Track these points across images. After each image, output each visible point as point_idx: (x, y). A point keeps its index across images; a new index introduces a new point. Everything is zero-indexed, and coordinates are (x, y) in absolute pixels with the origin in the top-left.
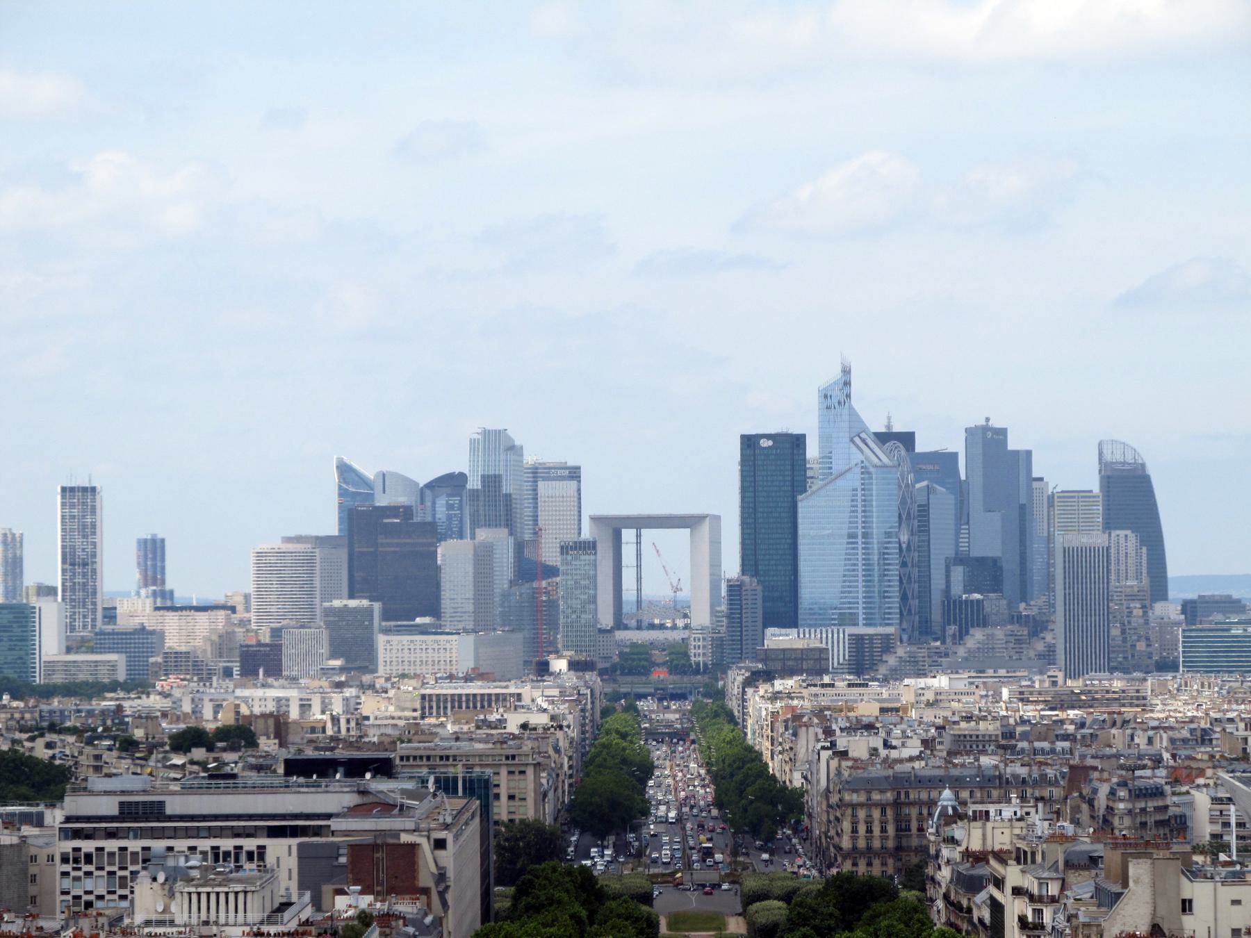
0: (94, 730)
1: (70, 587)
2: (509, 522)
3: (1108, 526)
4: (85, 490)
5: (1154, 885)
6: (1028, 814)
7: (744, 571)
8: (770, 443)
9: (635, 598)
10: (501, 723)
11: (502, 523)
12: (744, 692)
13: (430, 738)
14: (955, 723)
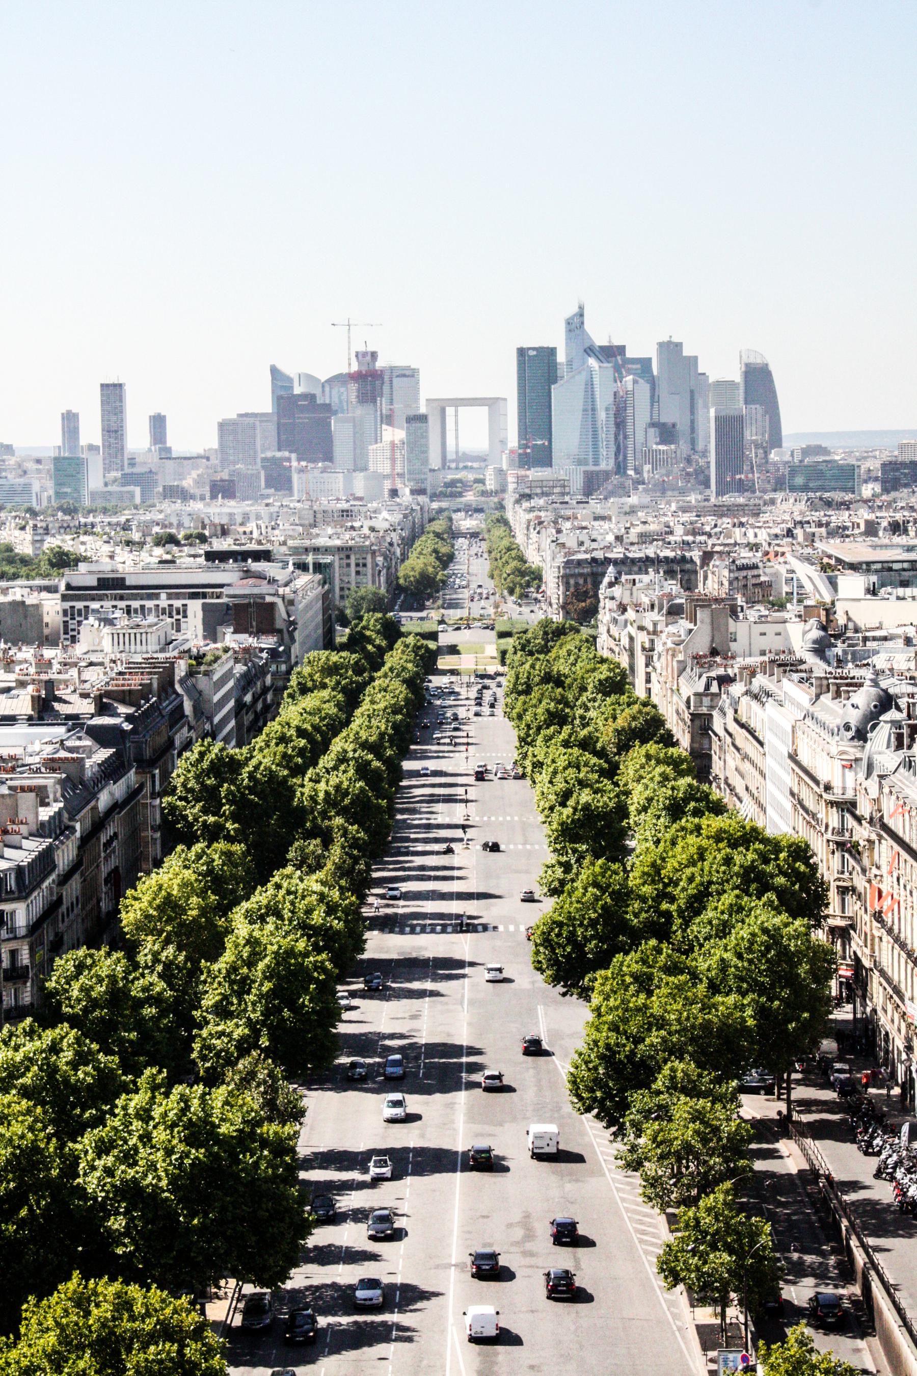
1: (107, 445)
4: (115, 385)
5: (712, 623)
8: (535, 353)
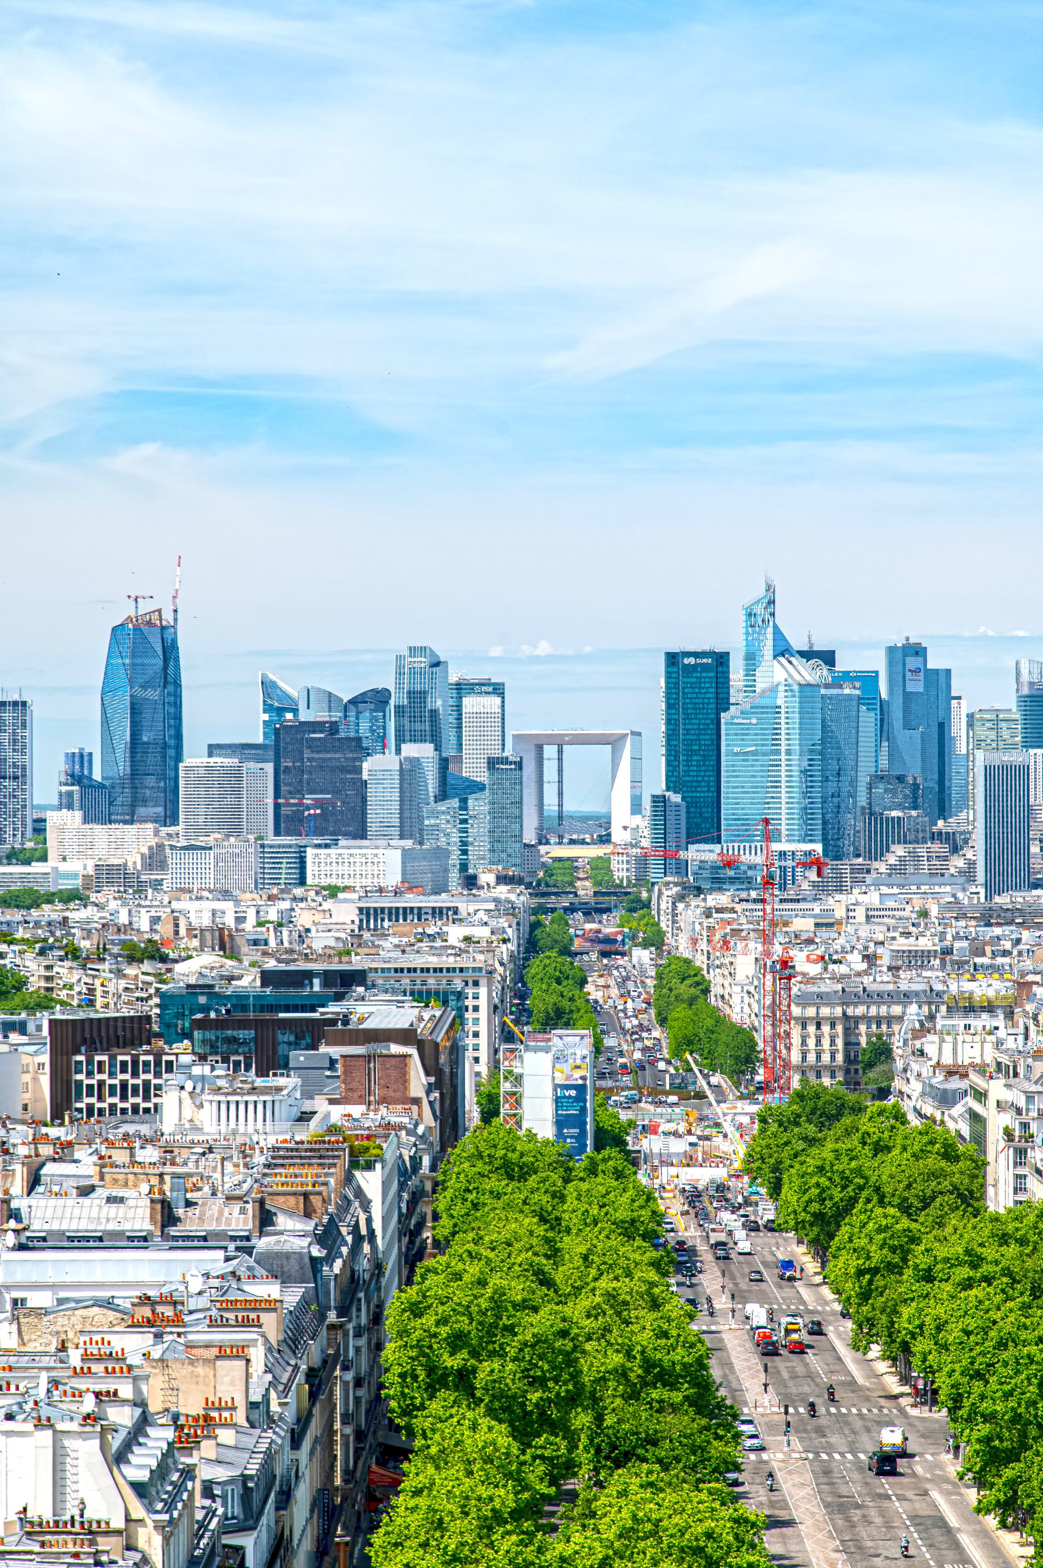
0: (45, 940)
2: (436, 739)
3: (1027, 744)
4: (15, 704)
6: (997, 1028)
7: (668, 789)
9: (557, 814)
10: (441, 935)
11: (428, 738)
12: (674, 907)
13: (373, 951)
14: (894, 938)
